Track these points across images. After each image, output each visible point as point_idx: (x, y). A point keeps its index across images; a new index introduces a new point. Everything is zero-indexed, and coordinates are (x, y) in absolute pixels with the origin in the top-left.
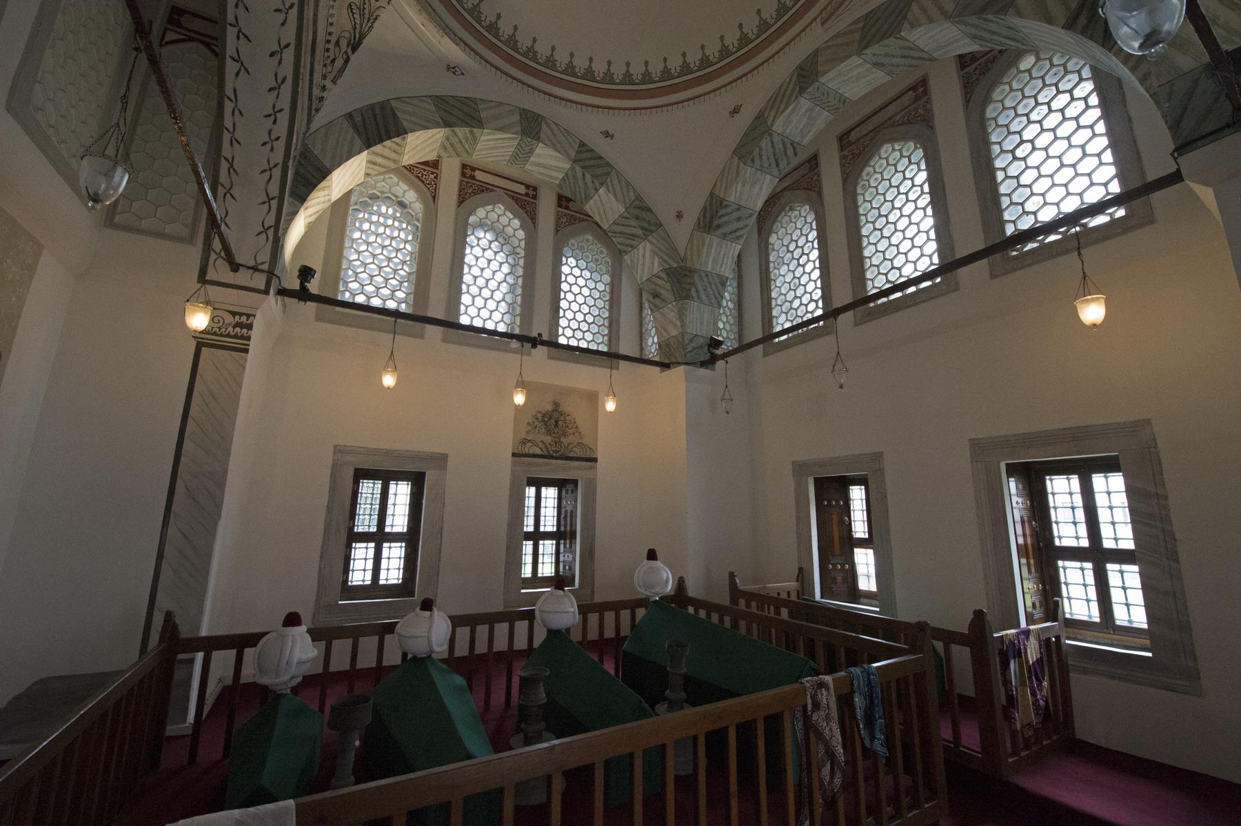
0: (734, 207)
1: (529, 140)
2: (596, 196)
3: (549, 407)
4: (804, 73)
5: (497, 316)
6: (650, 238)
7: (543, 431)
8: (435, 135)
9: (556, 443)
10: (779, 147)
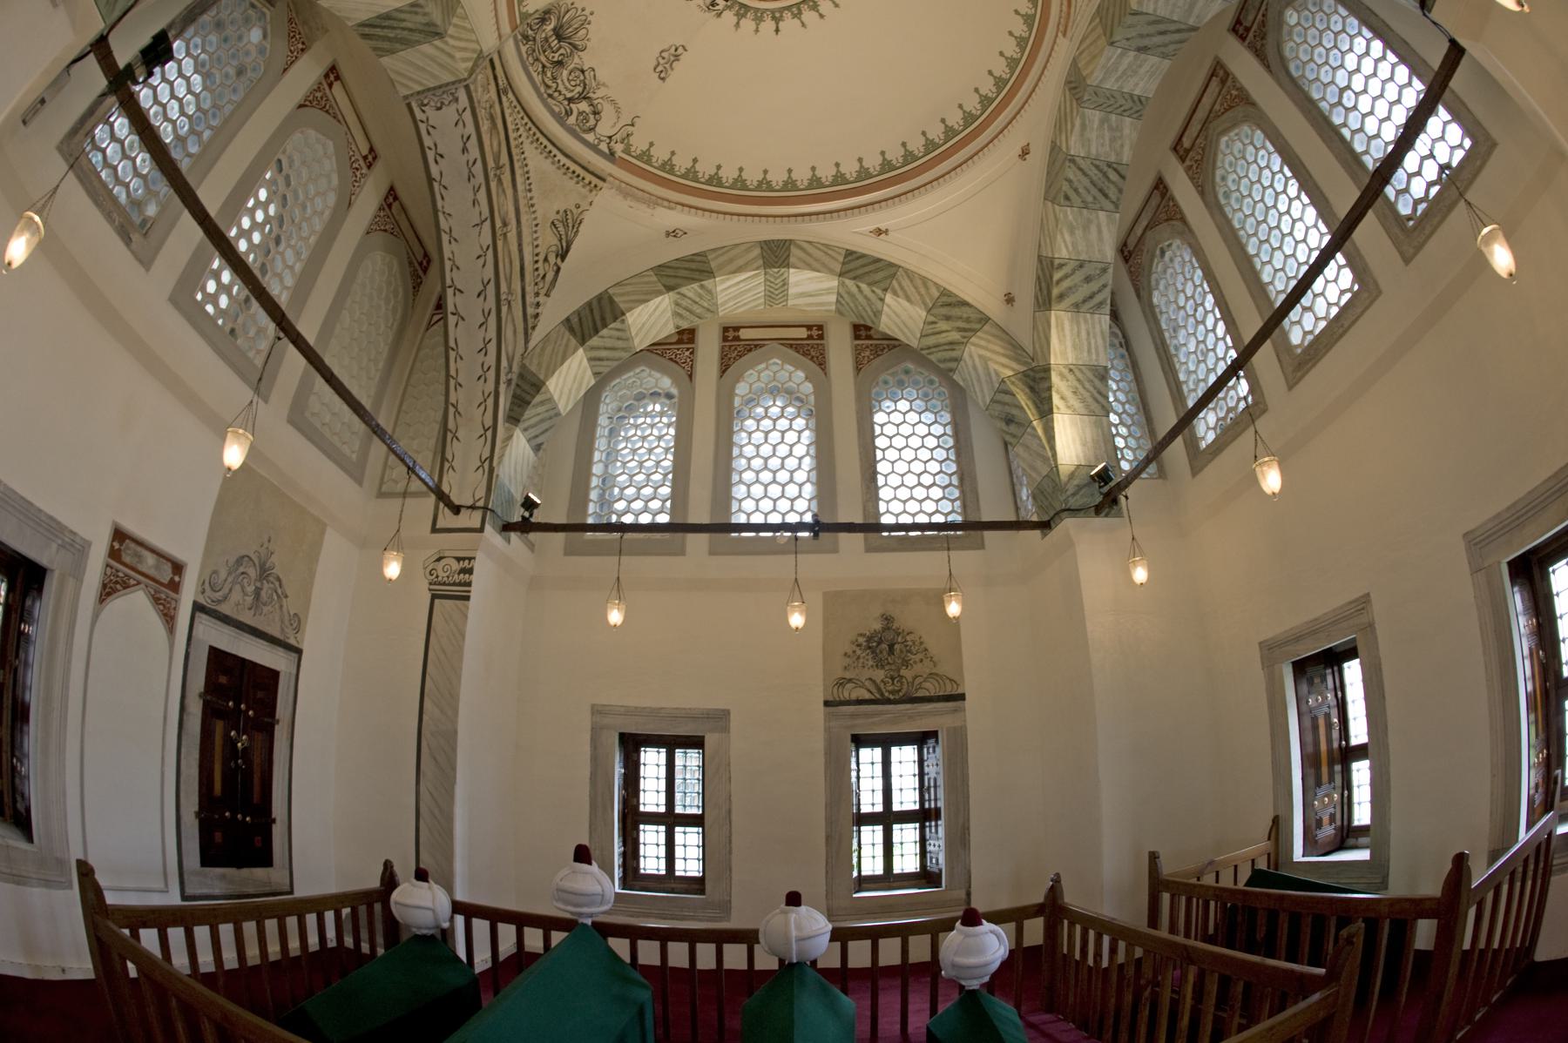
0: (1072, 264)
1: (776, 270)
2: (885, 308)
3: (877, 626)
4: (1073, 85)
6: (973, 339)
7: (871, 663)
8: (660, 303)
9: (893, 678)
10: (1093, 172)
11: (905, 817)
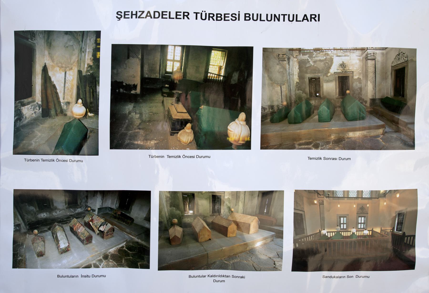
5: (356, 195)
11: (362, 223)
